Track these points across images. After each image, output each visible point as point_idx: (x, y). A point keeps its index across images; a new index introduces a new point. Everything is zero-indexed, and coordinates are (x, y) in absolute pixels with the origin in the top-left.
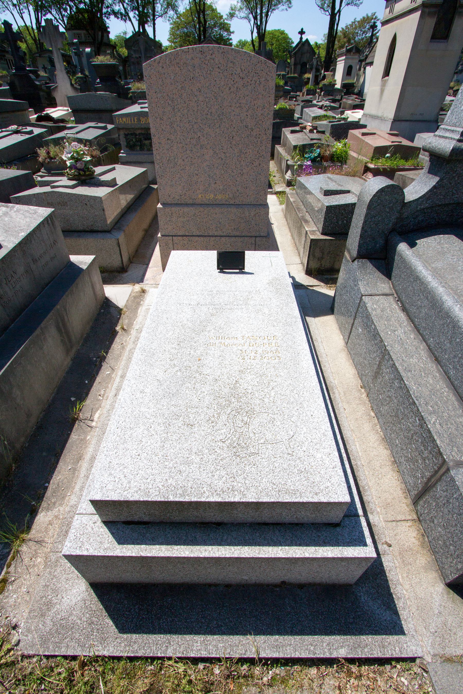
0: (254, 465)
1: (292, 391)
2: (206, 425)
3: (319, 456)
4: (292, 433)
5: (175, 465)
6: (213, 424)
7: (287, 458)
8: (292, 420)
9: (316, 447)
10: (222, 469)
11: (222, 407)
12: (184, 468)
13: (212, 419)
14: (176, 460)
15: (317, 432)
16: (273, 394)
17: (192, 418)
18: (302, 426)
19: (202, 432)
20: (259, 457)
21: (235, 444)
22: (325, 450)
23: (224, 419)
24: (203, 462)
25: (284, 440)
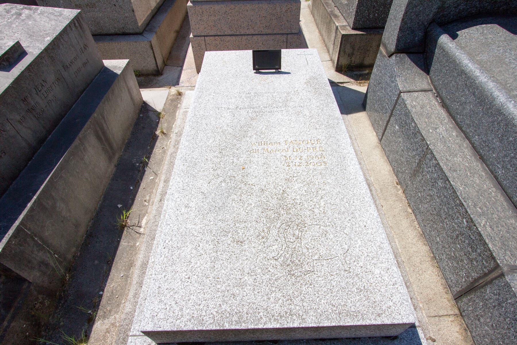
0: (311, 285)
1: (342, 200)
2: (257, 242)
3: (377, 271)
4: (346, 247)
5: (228, 288)
6: (263, 240)
7: (344, 275)
8: (345, 231)
9: (373, 261)
10: (277, 290)
11: (272, 221)
12: (237, 291)
13: (262, 234)
14: (229, 282)
15: (373, 244)
16: (322, 204)
17: (241, 234)
18: (357, 238)
19: (253, 249)
20: (315, 276)
21: (289, 261)
22: (383, 265)
23: (275, 234)
24: (256, 284)
25: (339, 255)
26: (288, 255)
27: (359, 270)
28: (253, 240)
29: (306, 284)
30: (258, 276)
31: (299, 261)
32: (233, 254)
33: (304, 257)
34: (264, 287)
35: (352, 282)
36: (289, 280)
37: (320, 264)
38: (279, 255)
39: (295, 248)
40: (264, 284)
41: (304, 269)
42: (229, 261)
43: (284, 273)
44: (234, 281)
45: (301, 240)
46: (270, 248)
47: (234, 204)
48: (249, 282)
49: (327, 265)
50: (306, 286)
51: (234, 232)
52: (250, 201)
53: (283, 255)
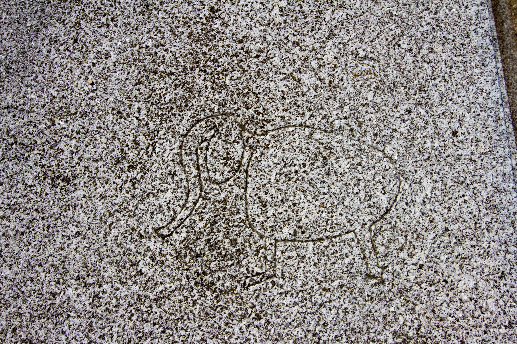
0: (259, 318)
1: (395, 42)
2: (113, 178)
3: (466, 282)
4: (383, 200)
5: (16, 323)
6: (133, 174)
7: (361, 292)
8: (388, 150)
9: (459, 249)
10: (158, 331)
11: (162, 110)
12: (42, 333)
13: (132, 154)
14: (19, 303)
15: (469, 193)
16: (330, 55)
17: (66, 154)
18: (421, 173)
19: (99, 205)
20: (275, 291)
21: (201, 243)
22: (489, 262)
23: (168, 156)
24: (99, 311)
26: (201, 224)
27: (412, 277)
28: (101, 174)
29: (243, 316)
30: (105, 286)
31: (234, 242)
32: (38, 216)
33: (248, 231)
34: (120, 321)
35: (384, 311)
36: (195, 303)
37: (294, 254)
38: (175, 224)
39: (225, 201)
40: (121, 311)
41: (243, 270)
42: (25, 238)
43: (184, 281)
44: (34, 300)
45: (247, 176)
46: (152, 199)
47: (54, 55)
48: (77, 306)
49: (315, 258)
50: (245, 322)
51: (47, 147)
52: (105, 42)
53: (187, 222)
